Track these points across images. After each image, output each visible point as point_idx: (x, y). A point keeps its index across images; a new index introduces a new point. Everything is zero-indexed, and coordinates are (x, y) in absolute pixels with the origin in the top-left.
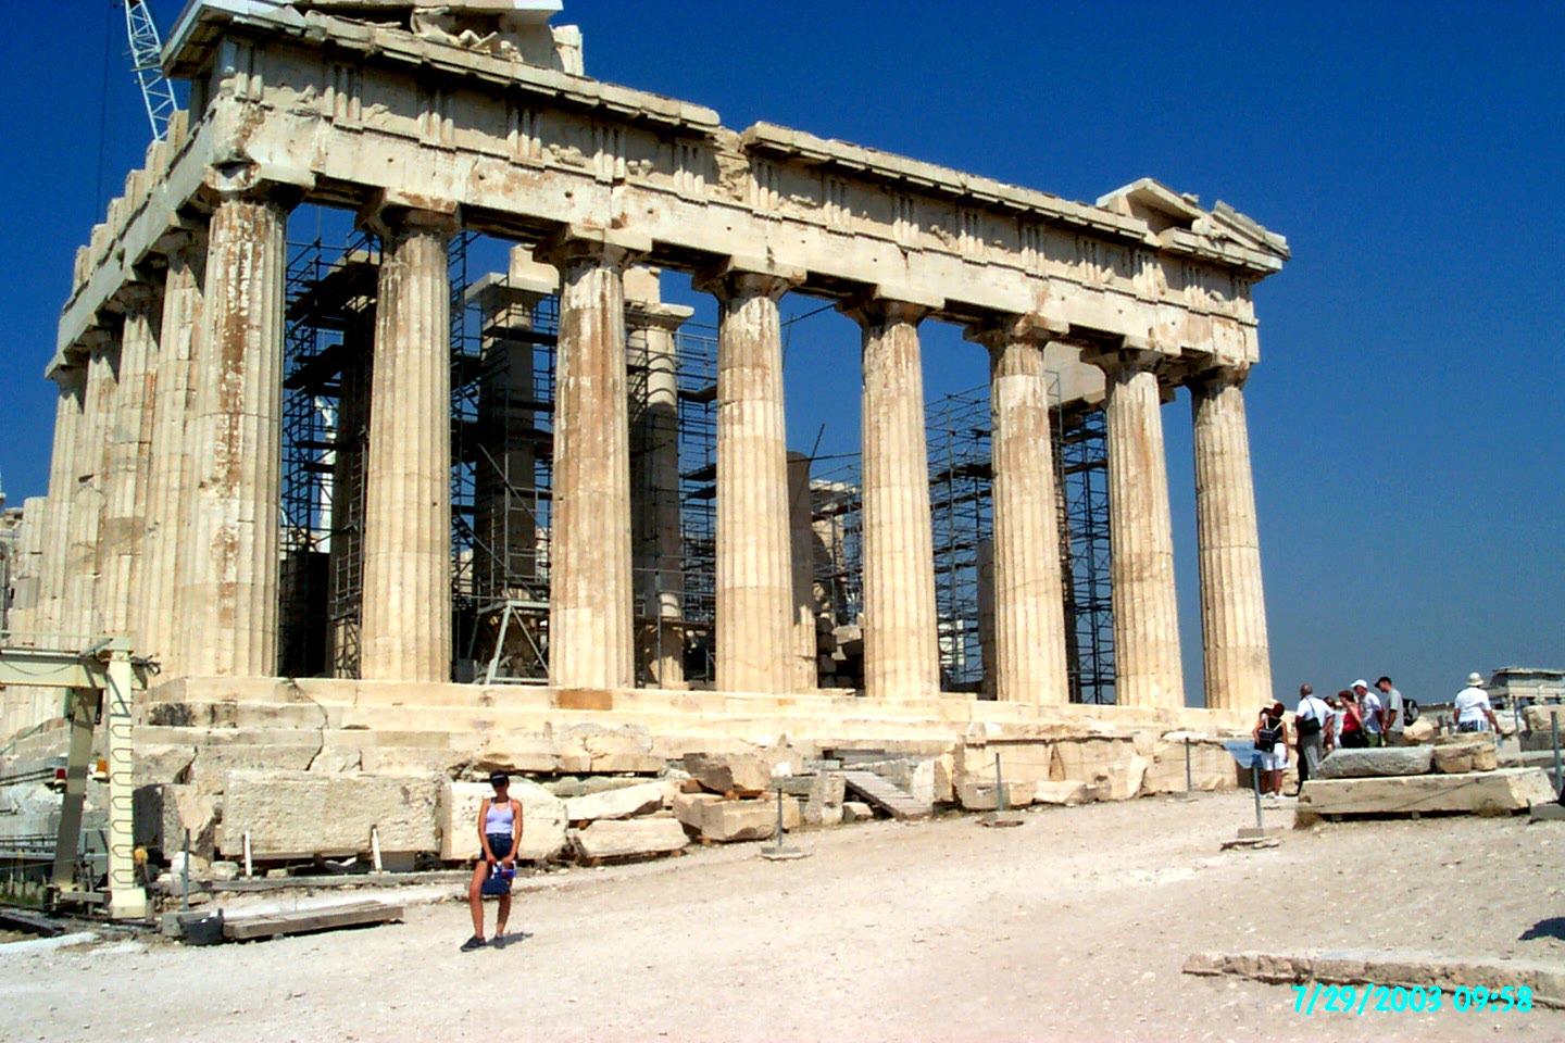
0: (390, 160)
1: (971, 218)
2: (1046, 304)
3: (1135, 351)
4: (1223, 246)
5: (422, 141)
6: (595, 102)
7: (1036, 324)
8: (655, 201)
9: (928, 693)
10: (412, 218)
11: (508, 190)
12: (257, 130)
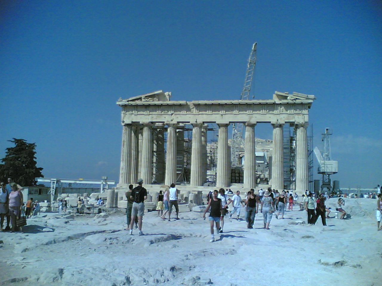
2: (252, 119)
3: (274, 124)
4: (296, 101)
7: (248, 123)
8: (178, 116)
9: (222, 186)
10: (144, 125)
11: (156, 119)
12: (125, 117)
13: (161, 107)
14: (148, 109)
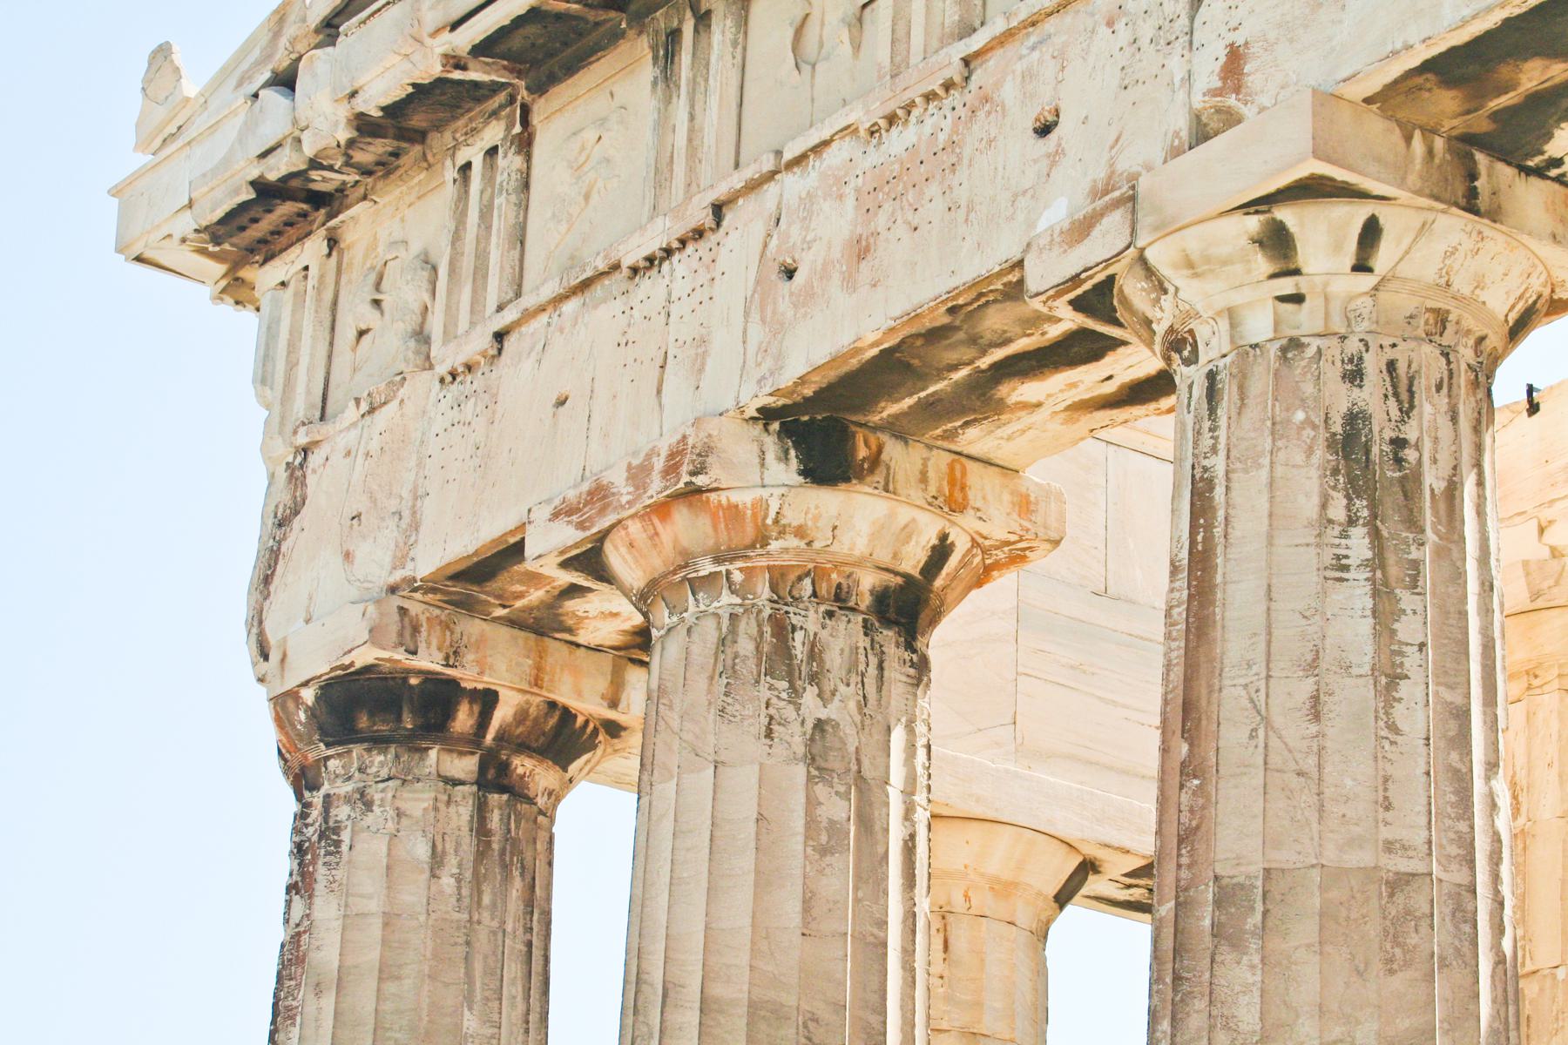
0: (561, 402)
5: (627, 262)
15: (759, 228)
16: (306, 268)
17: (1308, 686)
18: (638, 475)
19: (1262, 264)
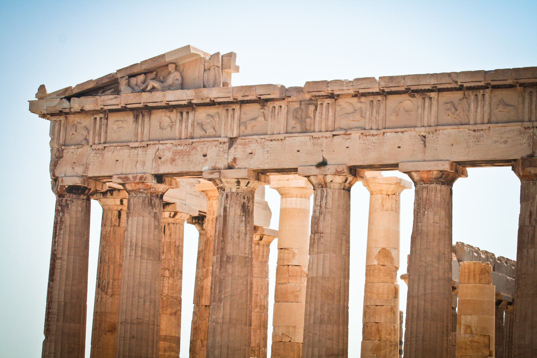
0: (117, 161)
1: (480, 97)
5: (131, 146)
6: (208, 101)
8: (253, 147)
10: (128, 187)
13: (191, 115)
14: (143, 121)
15: (155, 150)
16: (61, 120)
17: (238, 235)
18: (135, 178)
19: (236, 184)
